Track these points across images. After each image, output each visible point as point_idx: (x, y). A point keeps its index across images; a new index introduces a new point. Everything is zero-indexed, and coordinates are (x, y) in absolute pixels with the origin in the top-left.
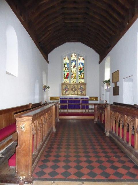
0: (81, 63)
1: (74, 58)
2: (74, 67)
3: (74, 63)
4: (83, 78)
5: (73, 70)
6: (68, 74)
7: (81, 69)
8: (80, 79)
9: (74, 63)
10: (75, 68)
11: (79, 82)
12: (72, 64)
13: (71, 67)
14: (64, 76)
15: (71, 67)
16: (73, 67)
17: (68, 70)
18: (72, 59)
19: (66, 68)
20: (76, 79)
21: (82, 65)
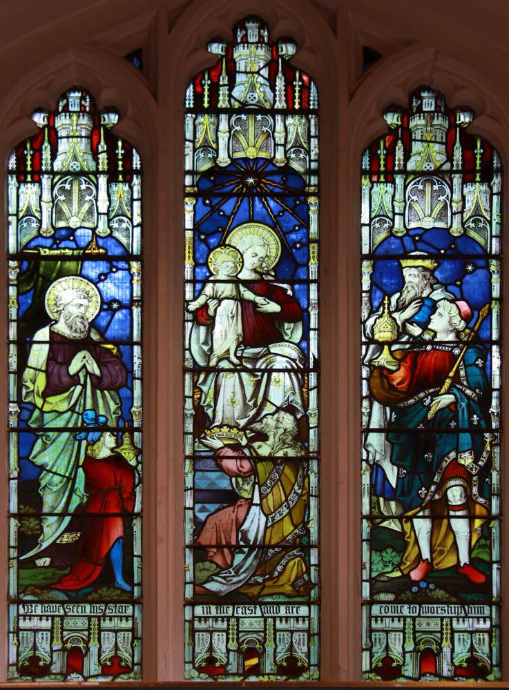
0: (420, 238)
1: (251, 115)
2: (260, 331)
3: (254, 245)
4: (463, 586)
5: (230, 397)
6: (109, 486)
8: (403, 591)
9: (254, 245)
10: (284, 353)
11: (389, 669)
12: (221, 263)
13: (195, 337)
14: (27, 539)
15: (195, 337)
16: (227, 331)
17: (108, 406)
18: (213, 141)
19: (62, 348)
20: (301, 592)
21: (455, 286)
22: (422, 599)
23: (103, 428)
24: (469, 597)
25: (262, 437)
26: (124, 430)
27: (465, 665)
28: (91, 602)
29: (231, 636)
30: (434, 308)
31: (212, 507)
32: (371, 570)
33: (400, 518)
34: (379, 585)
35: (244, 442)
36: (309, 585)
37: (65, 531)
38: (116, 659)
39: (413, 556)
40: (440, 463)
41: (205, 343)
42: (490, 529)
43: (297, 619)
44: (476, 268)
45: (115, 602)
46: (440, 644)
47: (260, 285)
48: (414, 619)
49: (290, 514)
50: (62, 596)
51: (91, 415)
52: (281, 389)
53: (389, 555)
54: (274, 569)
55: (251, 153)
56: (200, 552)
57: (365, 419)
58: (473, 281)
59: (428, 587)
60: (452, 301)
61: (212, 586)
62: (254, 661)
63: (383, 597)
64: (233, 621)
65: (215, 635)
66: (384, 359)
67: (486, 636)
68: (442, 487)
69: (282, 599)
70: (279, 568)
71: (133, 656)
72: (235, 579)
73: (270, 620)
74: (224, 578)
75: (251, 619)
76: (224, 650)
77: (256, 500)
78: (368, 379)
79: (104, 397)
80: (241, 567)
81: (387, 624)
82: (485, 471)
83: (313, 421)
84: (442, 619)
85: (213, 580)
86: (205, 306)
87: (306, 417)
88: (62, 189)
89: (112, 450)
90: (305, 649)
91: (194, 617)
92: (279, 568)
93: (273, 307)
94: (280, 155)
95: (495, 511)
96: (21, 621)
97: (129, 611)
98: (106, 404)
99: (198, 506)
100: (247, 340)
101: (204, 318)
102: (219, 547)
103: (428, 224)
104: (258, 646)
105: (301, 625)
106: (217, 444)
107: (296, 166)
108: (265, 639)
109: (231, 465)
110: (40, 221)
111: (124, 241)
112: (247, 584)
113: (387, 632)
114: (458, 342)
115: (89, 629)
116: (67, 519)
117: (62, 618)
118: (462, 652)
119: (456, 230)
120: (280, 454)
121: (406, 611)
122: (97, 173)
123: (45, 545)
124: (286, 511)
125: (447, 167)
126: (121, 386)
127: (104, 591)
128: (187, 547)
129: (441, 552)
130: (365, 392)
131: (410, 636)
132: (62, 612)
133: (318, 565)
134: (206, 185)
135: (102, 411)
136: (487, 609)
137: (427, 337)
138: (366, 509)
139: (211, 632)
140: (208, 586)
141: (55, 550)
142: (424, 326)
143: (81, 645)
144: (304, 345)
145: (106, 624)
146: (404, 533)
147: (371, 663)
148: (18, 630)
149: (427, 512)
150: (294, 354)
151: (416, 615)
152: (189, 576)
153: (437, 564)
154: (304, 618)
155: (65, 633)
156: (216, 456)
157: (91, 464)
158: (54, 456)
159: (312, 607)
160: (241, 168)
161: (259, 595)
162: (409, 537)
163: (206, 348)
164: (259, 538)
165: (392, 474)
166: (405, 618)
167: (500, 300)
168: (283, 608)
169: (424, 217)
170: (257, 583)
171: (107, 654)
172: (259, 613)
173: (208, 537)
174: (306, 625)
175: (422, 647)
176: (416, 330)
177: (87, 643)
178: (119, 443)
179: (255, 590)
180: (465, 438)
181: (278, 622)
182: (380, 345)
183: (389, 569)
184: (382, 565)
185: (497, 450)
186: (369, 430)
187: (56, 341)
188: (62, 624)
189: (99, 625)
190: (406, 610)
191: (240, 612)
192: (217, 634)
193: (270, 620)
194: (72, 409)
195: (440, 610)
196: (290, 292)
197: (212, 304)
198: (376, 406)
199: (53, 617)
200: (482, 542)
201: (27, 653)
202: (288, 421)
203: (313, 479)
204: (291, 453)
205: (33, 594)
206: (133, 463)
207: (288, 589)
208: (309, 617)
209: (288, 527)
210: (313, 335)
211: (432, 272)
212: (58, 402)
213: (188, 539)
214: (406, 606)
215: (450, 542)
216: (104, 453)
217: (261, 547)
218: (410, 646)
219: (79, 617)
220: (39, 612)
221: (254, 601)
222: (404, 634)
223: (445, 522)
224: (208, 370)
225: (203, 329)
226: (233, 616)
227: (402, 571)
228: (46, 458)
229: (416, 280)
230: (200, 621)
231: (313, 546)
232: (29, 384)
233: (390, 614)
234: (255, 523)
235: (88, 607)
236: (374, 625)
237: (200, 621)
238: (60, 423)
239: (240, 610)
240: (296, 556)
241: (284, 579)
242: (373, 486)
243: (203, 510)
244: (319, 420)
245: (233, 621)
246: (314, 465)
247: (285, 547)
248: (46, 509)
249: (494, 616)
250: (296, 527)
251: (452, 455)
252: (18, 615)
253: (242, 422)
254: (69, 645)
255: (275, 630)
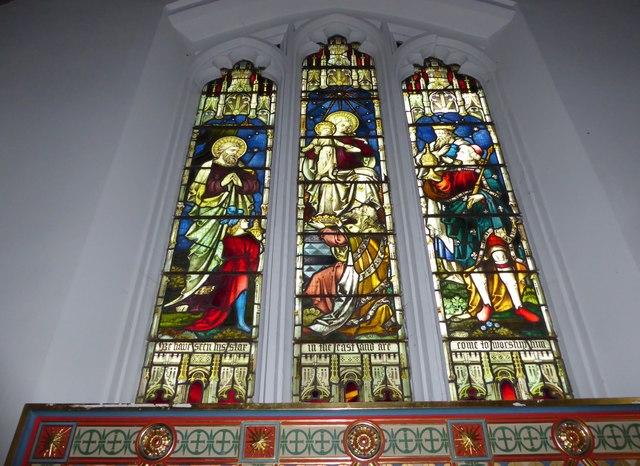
2: (347, 162)
3: (342, 121)
5: (330, 197)
7: (459, 180)
8: (473, 330)
10: (365, 173)
12: (323, 129)
14: (172, 292)
15: (306, 167)
16: (326, 162)
19: (218, 172)
22: (490, 336)
23: (241, 217)
24: (529, 334)
25: (353, 221)
26: (254, 218)
27: (541, 394)
28: (215, 341)
29: (332, 371)
30: (458, 149)
31: (317, 267)
32: (445, 314)
33: (461, 273)
34: (453, 325)
35: (340, 224)
36: (396, 327)
37: (203, 285)
38: (232, 392)
39: (477, 302)
40: (482, 236)
41: (313, 168)
42: (531, 281)
43: (389, 355)
44: (480, 129)
45: (236, 341)
46: (515, 375)
47: (347, 138)
48: (488, 353)
49: (376, 272)
50: (193, 336)
51: (233, 209)
52: (363, 194)
53: (457, 301)
54: (367, 313)
55: (339, 83)
56: (307, 300)
57: (424, 210)
58: (480, 136)
59: (493, 326)
60: (469, 145)
61: (317, 328)
62: (354, 394)
63: (457, 335)
64: (334, 357)
65: (319, 370)
66: (431, 175)
67: (553, 367)
68: (487, 252)
69: (374, 338)
70: (371, 313)
71: (247, 390)
72: (336, 322)
73: (366, 356)
74: (326, 321)
75: (349, 354)
76: (327, 383)
77: (350, 262)
78: (422, 187)
79: (243, 198)
80: (340, 313)
81: (467, 358)
82: (517, 241)
83: (388, 212)
84: (512, 352)
85: (317, 323)
86: (313, 149)
87: (383, 209)
88: (231, 99)
89: (245, 230)
90: (398, 382)
91: (301, 354)
92: (371, 313)
93: (356, 150)
94: (355, 83)
95: (531, 268)
96: (155, 358)
97: (247, 349)
98: (244, 202)
99: (306, 267)
100: (339, 166)
101: (312, 156)
102: (322, 296)
103: (446, 110)
104: (357, 379)
105: (392, 360)
106: (321, 226)
107: (365, 88)
108: (362, 373)
109: (332, 239)
110: (216, 113)
111: (264, 120)
112: (346, 326)
113: (467, 365)
114: (477, 164)
115: (211, 365)
116: (206, 277)
117: (190, 354)
118: (536, 384)
119: (462, 112)
120: (367, 231)
121: (480, 348)
122: (252, 92)
123: (186, 295)
124: (373, 270)
125: (450, 87)
126: (255, 192)
127: (228, 332)
128: (297, 296)
129: (498, 299)
130: (421, 193)
131: (487, 367)
132: (191, 350)
133: (402, 310)
134: (313, 96)
135: (241, 207)
136: (546, 342)
137: (457, 163)
138: (434, 268)
139: (315, 367)
140: (312, 327)
141: (194, 300)
142: (454, 157)
143: (203, 379)
144: (378, 168)
145: (227, 360)
146: (466, 285)
147: (458, 395)
148: (152, 364)
149: (480, 269)
150: (372, 174)
151: (489, 349)
152: (298, 319)
153: (497, 307)
154: (394, 354)
155: (191, 368)
156: (320, 233)
157: (229, 240)
158: (202, 234)
159: (401, 344)
160: (331, 90)
161: (356, 334)
162: (471, 287)
163: (313, 171)
164: (354, 288)
165: (449, 243)
166: (480, 352)
167: (498, 144)
168: (376, 345)
169: (443, 107)
170: (353, 325)
171: (225, 387)
172: (356, 350)
173: (311, 290)
174: (397, 361)
175: (500, 378)
176: (449, 161)
177: (208, 377)
178: (250, 226)
179: (353, 331)
180: (497, 221)
181: (373, 358)
182: (427, 168)
183: (460, 312)
184: (454, 308)
185: (521, 227)
186: (427, 216)
187: (216, 168)
188: (189, 360)
189: (220, 361)
190: (479, 345)
191: (340, 348)
192: (320, 369)
193: (366, 356)
194: (220, 206)
195: (508, 345)
196: (366, 142)
197: (317, 149)
198: (430, 201)
199: (183, 354)
200: (528, 290)
201: (155, 386)
202: (370, 212)
203: (392, 249)
204: (374, 230)
205: (169, 334)
206: (259, 238)
207: (379, 329)
208: (399, 352)
209: (376, 282)
210: (382, 164)
211: (453, 131)
212: (212, 201)
213: (298, 290)
214: (479, 342)
215: (503, 291)
216: (240, 232)
217: (356, 296)
218: (489, 378)
219: (203, 353)
220: (172, 350)
221: (351, 340)
222: (482, 366)
223: (496, 276)
224: (314, 183)
225: (311, 162)
226: (334, 353)
227: (470, 314)
228: (198, 235)
229: (444, 136)
230: (306, 358)
231: (397, 295)
232: (194, 191)
233: (466, 349)
234: (350, 279)
235: (213, 344)
236: (455, 359)
237: (306, 358)
238: (211, 213)
239: (340, 348)
240: (384, 304)
241: (375, 320)
242: (437, 253)
243: (309, 270)
244: (392, 210)
245: (334, 357)
246: (391, 239)
247: (376, 296)
248: (191, 270)
249: (554, 349)
250: (381, 281)
251: (490, 230)
252: (155, 352)
253: (338, 212)
254: (192, 379)
255: (371, 365)
